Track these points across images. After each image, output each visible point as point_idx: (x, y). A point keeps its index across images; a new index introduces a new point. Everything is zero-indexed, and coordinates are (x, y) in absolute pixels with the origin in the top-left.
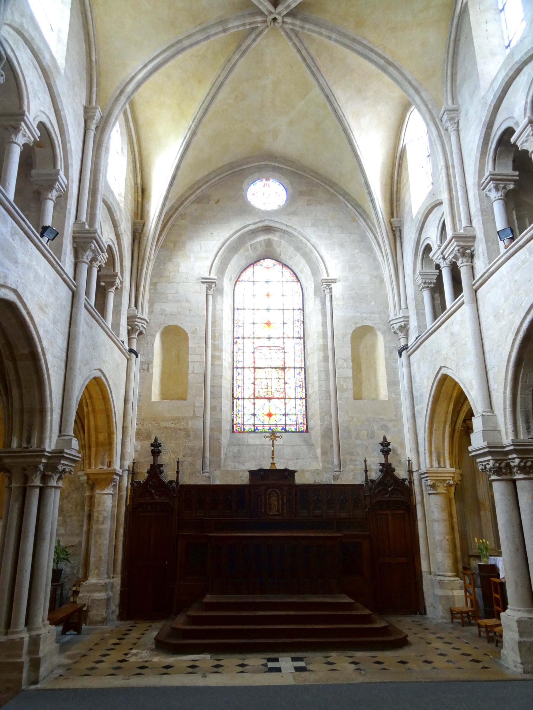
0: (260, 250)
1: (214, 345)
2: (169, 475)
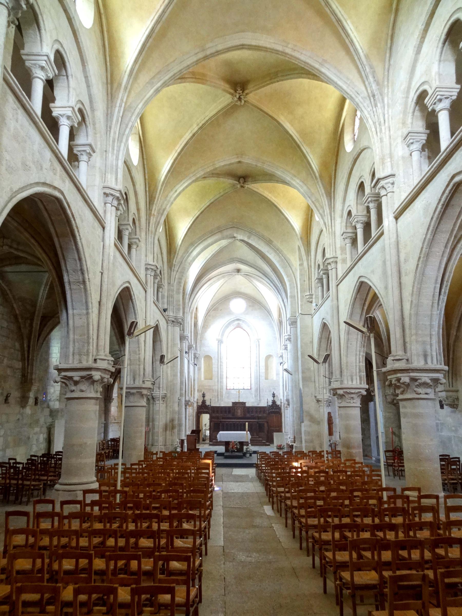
0: (235, 326)
1: (220, 361)
2: (208, 403)
